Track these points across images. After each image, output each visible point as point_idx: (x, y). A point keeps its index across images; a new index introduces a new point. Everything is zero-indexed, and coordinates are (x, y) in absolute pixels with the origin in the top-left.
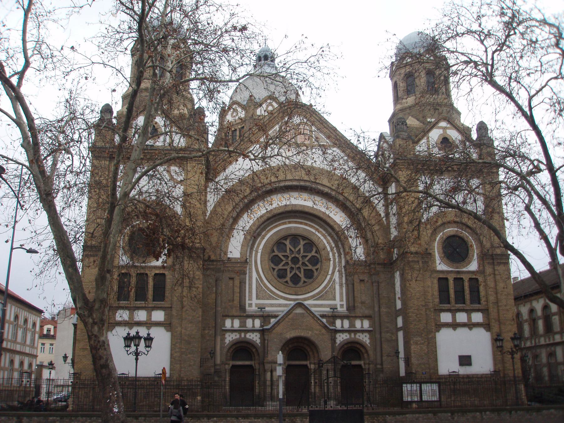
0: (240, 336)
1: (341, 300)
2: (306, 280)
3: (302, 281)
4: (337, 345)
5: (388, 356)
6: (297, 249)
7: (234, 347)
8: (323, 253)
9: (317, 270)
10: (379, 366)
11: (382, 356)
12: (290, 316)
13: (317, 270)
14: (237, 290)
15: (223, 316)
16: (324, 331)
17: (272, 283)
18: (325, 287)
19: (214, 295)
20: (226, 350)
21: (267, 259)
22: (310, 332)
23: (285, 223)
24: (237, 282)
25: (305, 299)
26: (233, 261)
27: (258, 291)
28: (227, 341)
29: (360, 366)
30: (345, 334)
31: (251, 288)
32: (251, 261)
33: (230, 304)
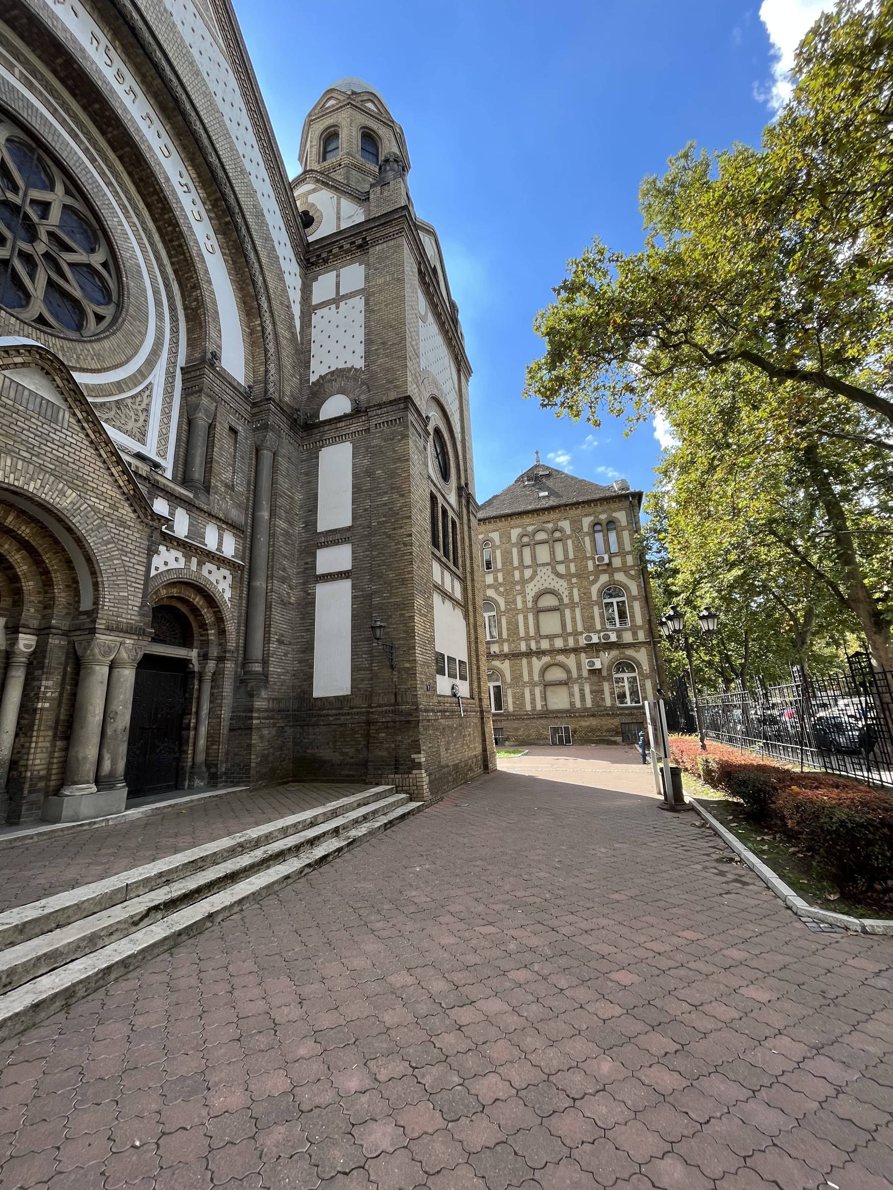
1: (163, 454)
5: (280, 642)
9: (99, 318)
10: (257, 668)
11: (267, 640)
16: (126, 511)
18: (119, 386)
22: (72, 495)
29: (184, 663)
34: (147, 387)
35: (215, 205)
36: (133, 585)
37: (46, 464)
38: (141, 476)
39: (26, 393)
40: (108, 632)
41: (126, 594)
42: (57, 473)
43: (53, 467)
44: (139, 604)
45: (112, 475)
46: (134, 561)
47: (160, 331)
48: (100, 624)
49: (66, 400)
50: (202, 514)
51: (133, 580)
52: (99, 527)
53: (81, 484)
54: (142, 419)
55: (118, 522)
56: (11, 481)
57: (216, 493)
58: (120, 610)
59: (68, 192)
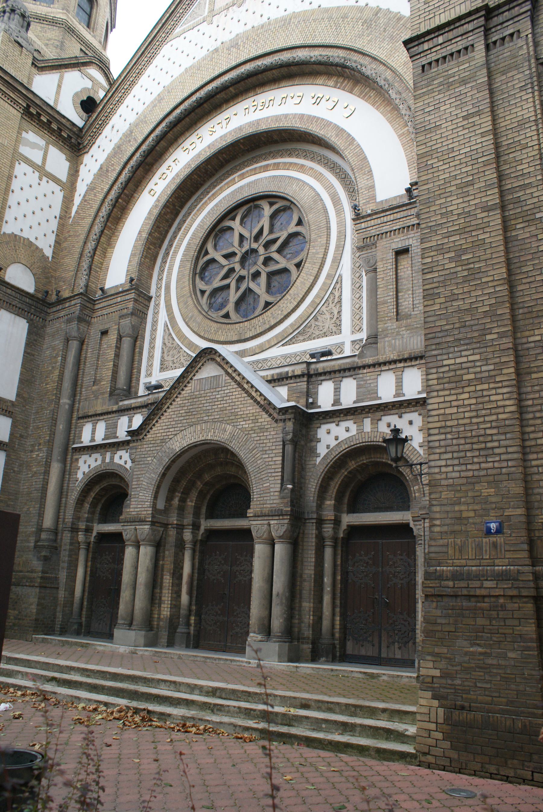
0: (103, 460)
2: (270, 299)
3: (262, 304)
4: (319, 460)
6: (255, 231)
7: (97, 489)
8: (310, 218)
12: (187, 391)
13: (298, 265)
14: (111, 354)
15: (79, 418)
16: (264, 418)
17: (193, 325)
18: (314, 304)
19: (57, 373)
20: (73, 496)
21: (187, 272)
22: (229, 428)
23: (234, 182)
24: (112, 337)
25: (262, 349)
26: (113, 292)
27: (166, 352)
28: (80, 476)
30: (344, 424)
31: (152, 347)
32: (159, 288)
33: (94, 388)
34: (337, 282)
35: (340, 75)
36: (274, 474)
37: (216, 417)
38: (299, 376)
39: (204, 380)
40: (256, 518)
41: (268, 484)
42: (221, 419)
43: (218, 417)
44: (278, 489)
45: (252, 398)
46: (273, 455)
47: (341, 224)
48: (250, 513)
49: (223, 368)
50: (372, 369)
51: (273, 471)
52: (247, 440)
53: (233, 417)
54: (336, 313)
55: (259, 431)
56: (201, 438)
57: (386, 336)
58: (265, 498)
59: (271, 204)
